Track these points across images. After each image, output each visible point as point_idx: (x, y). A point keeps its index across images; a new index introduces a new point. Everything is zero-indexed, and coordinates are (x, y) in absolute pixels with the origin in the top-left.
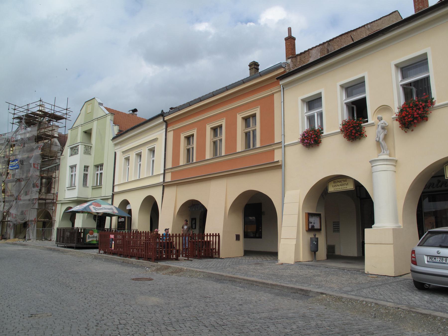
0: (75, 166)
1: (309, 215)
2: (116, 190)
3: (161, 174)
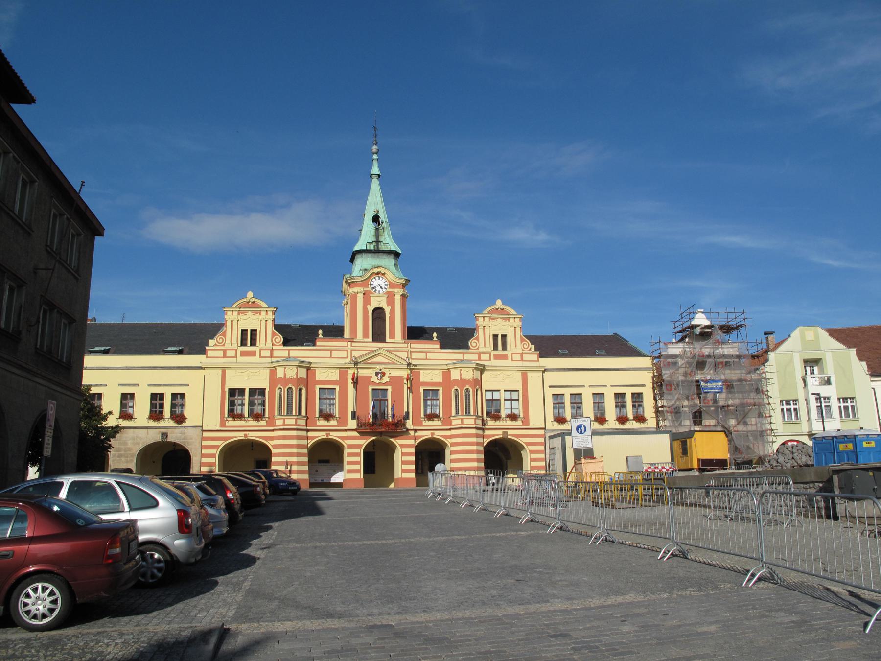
0: (828, 398)
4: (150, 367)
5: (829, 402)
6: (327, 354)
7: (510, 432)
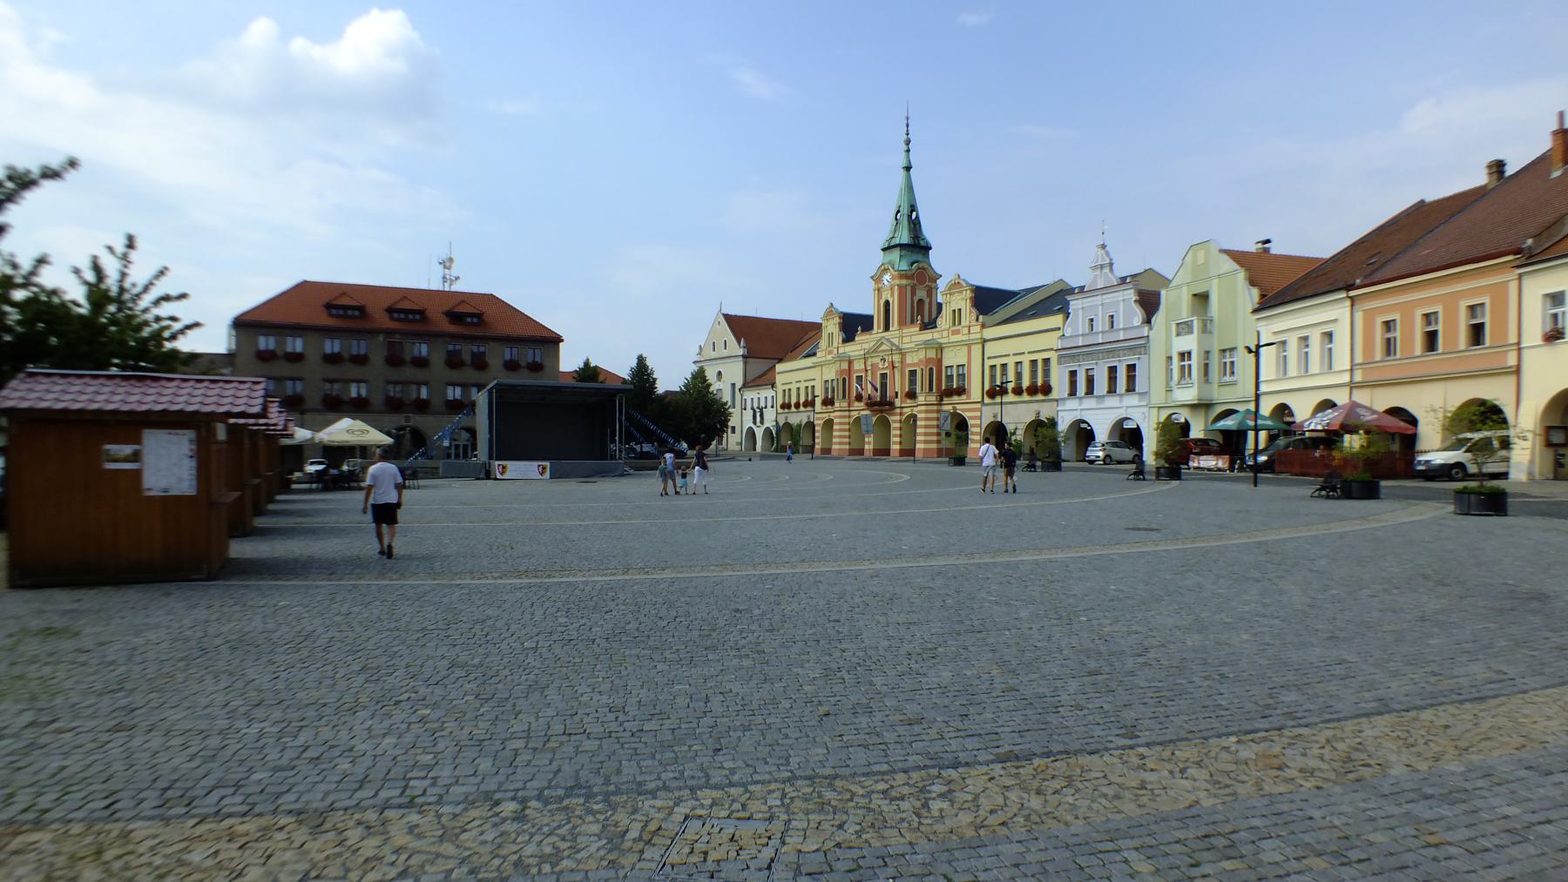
1: (1549, 429)
2: (1263, 388)
6: (858, 347)
7: (958, 407)
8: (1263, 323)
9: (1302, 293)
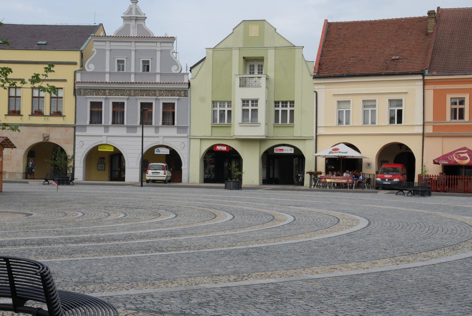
2: (320, 131)
3: (421, 125)
4: (4, 63)
5: (257, 105)
8: (323, 86)
9: (353, 71)
